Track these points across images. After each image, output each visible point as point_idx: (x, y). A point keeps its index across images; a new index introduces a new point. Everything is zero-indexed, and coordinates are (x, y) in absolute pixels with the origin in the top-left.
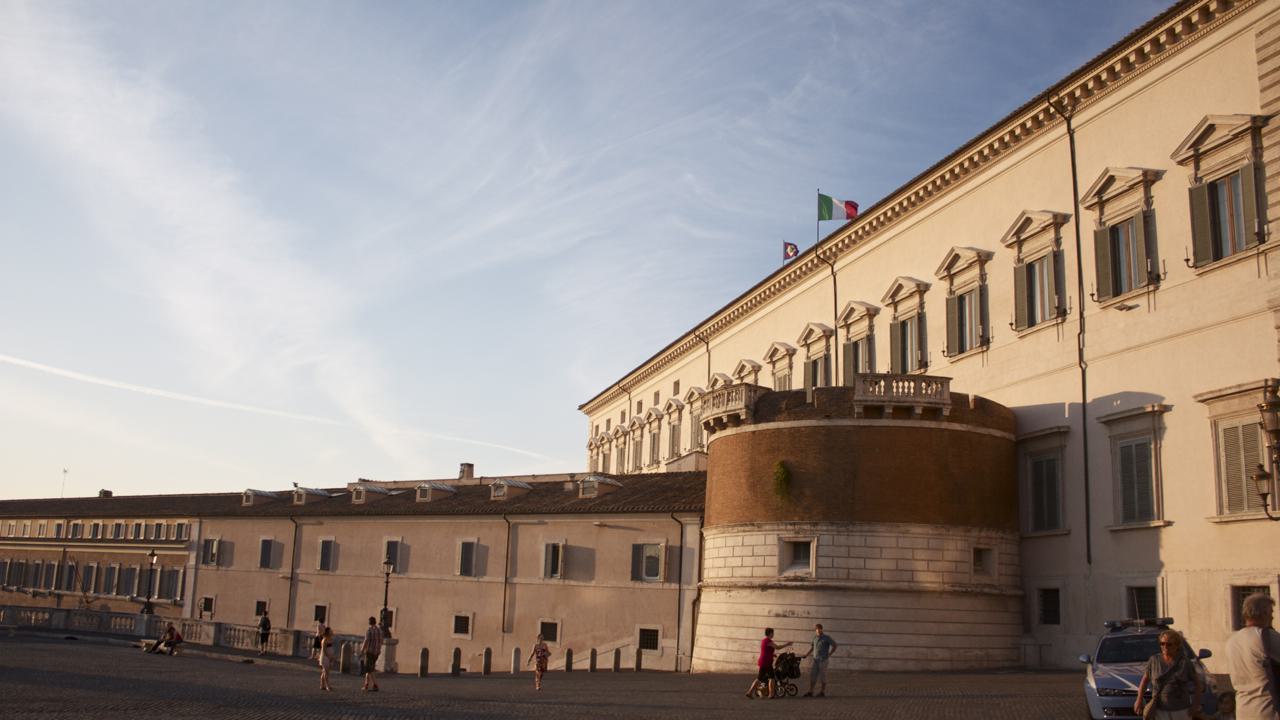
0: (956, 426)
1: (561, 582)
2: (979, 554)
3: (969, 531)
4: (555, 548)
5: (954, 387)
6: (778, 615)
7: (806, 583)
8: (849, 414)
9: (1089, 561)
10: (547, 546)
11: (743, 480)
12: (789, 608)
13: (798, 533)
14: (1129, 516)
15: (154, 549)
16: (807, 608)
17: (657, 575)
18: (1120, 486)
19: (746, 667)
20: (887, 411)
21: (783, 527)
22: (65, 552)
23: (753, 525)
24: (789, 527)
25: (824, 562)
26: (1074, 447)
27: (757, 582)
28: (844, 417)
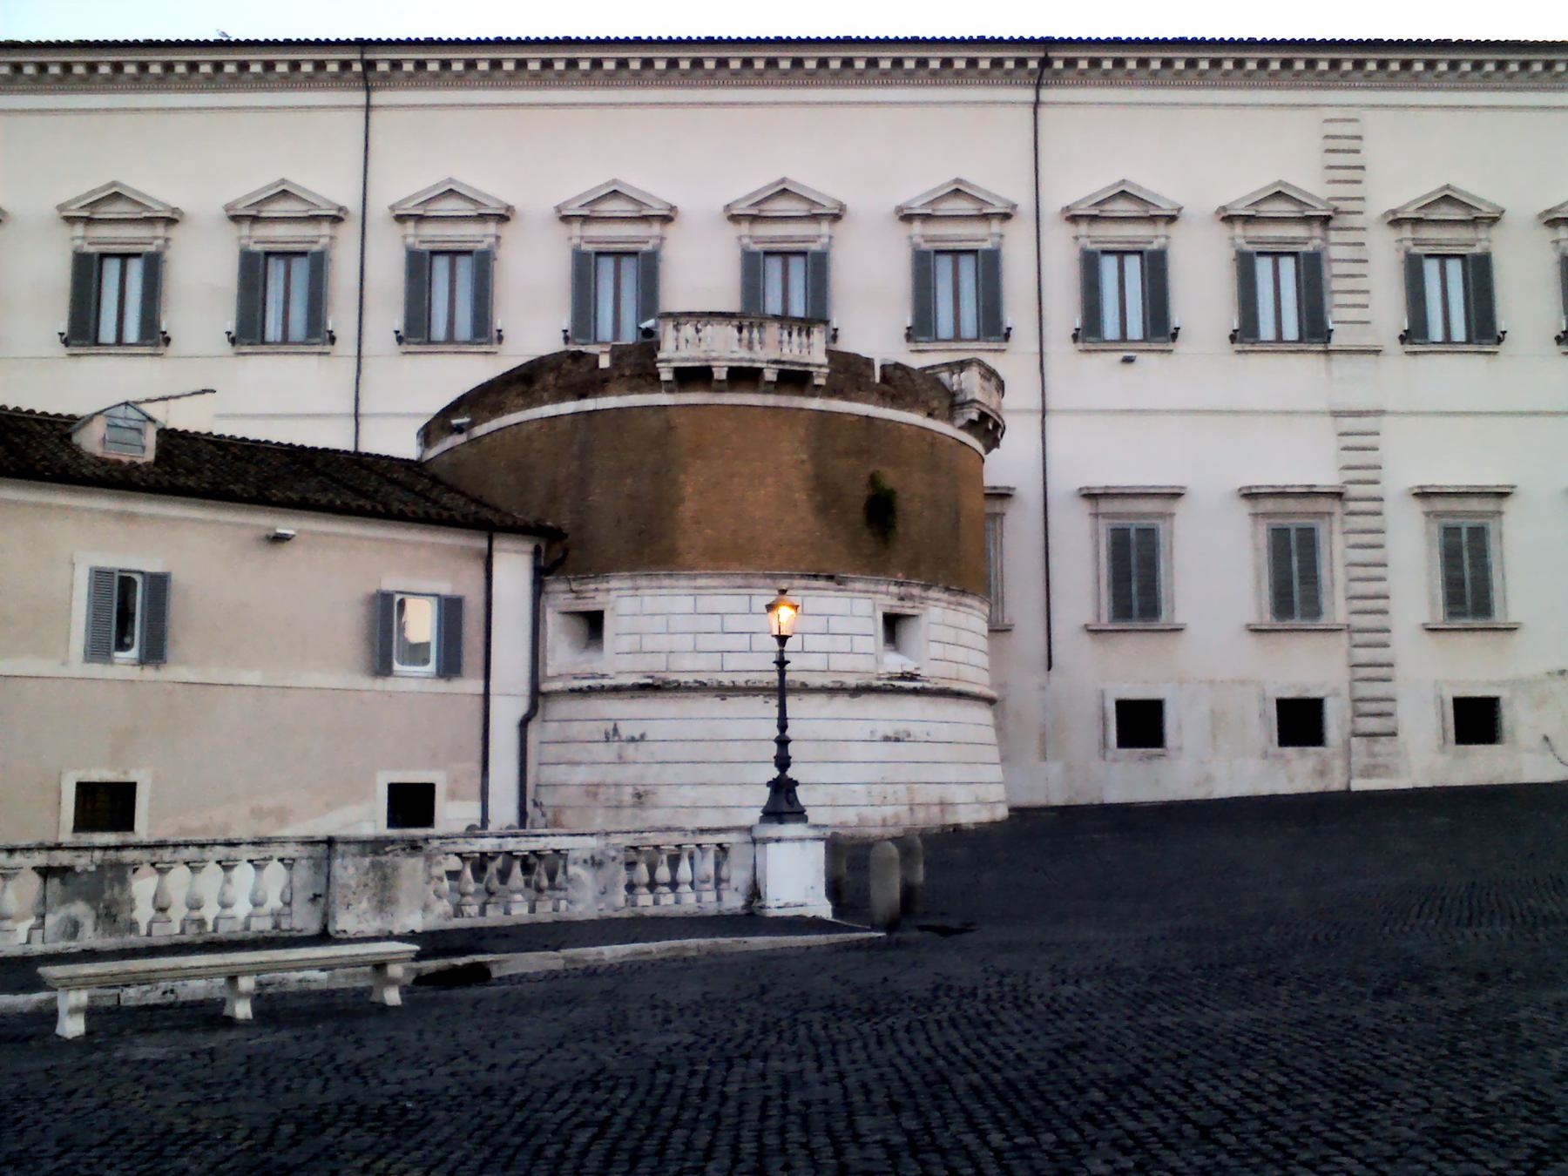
1: (136, 673)
4: (126, 583)
6: (887, 739)
8: (950, 419)
9: (1049, 667)
10: (100, 576)
14: (1122, 609)
25: (936, 650)
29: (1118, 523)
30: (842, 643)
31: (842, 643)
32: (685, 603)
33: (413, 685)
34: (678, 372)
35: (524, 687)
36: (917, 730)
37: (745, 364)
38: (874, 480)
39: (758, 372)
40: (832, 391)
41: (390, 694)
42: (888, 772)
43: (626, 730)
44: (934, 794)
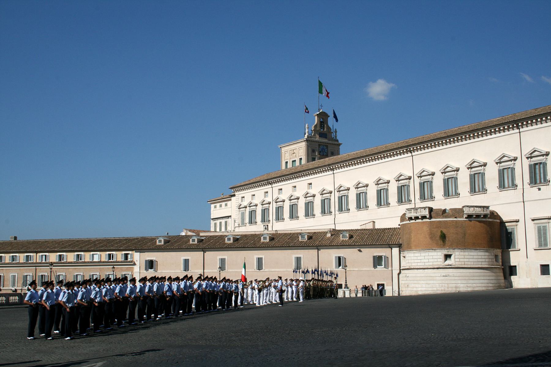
0: (490, 220)
2: (496, 256)
3: (494, 250)
4: (339, 258)
5: (491, 209)
6: (444, 276)
7: (453, 266)
8: (463, 217)
9: (527, 258)
10: (336, 257)
11: (427, 236)
12: (447, 274)
13: (448, 252)
14: (540, 245)
15: (114, 265)
16: (453, 274)
17: (382, 265)
18: (537, 237)
19: (434, 292)
20: (474, 216)
21: (444, 250)
22: (36, 269)
23: (433, 249)
24: (445, 250)
25: (457, 260)
26: (521, 225)
27: (436, 267)
28: (460, 217)
29: (539, 225)
30: (436, 260)
31: (436, 260)
32: (413, 255)
33: (380, 269)
34: (415, 217)
35: (399, 269)
36: (451, 274)
37: (416, 216)
38: (442, 232)
39: (418, 217)
40: (431, 217)
41: (377, 271)
42: (444, 282)
43: (407, 276)
44: (454, 285)
